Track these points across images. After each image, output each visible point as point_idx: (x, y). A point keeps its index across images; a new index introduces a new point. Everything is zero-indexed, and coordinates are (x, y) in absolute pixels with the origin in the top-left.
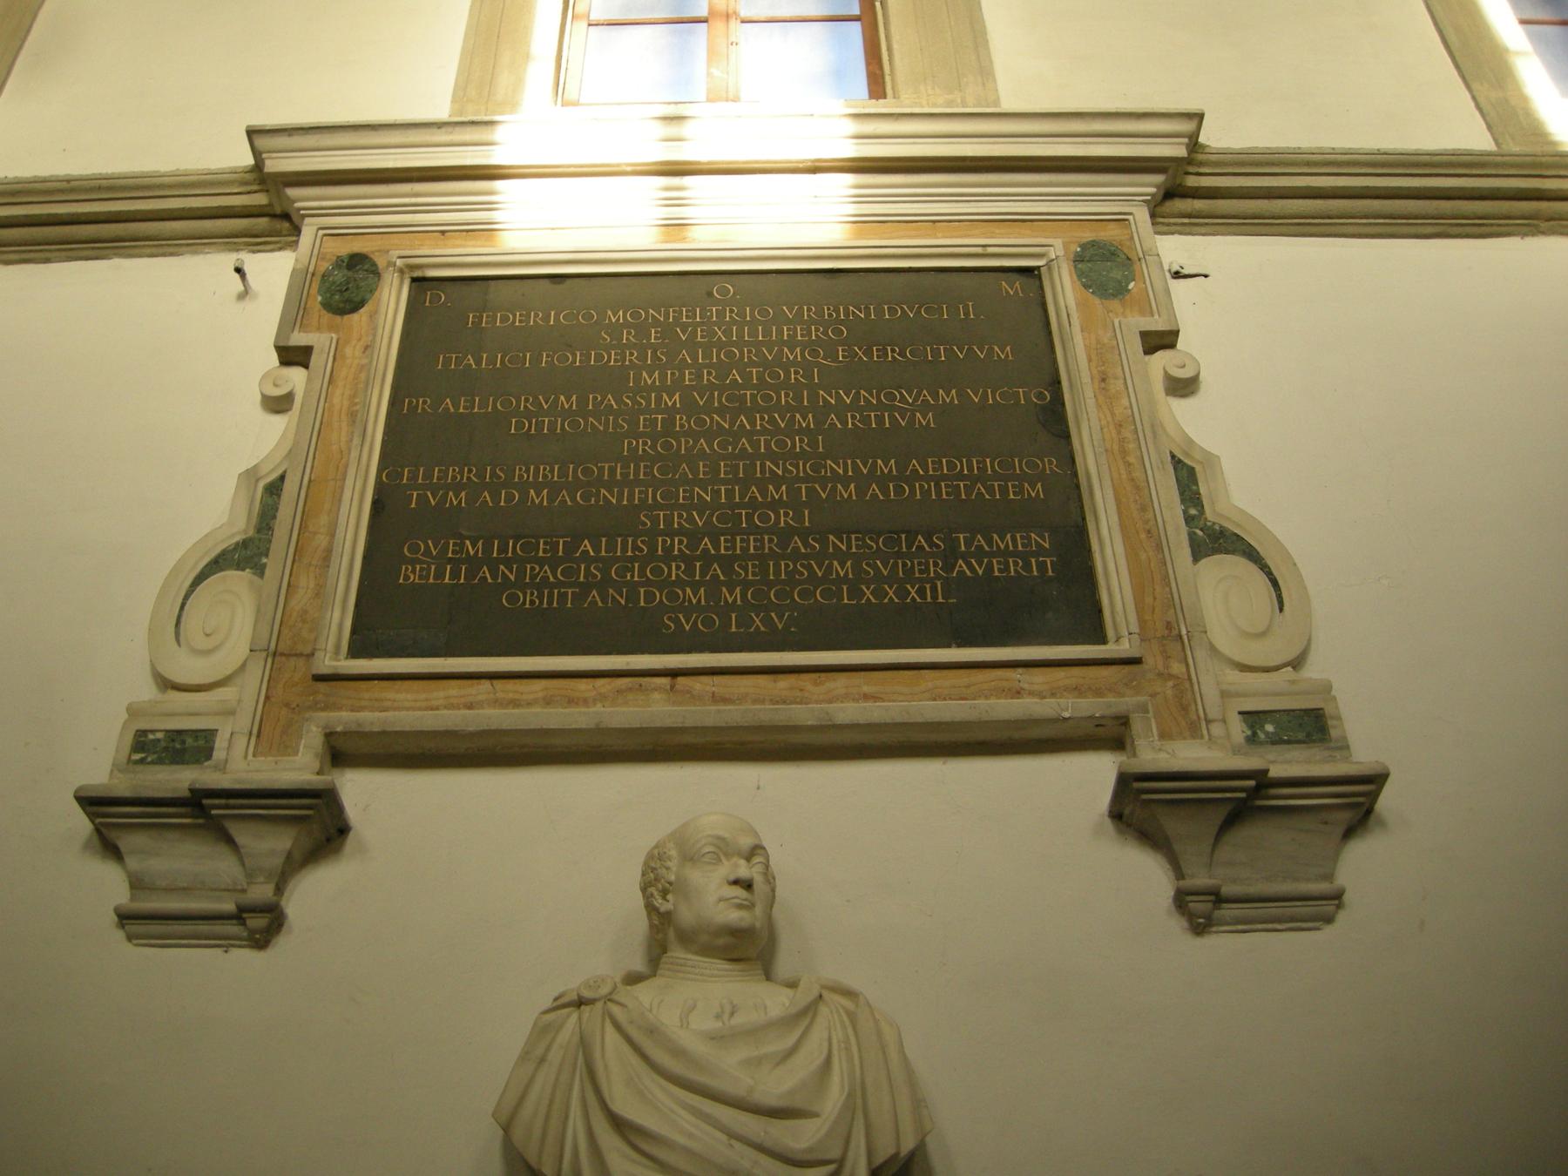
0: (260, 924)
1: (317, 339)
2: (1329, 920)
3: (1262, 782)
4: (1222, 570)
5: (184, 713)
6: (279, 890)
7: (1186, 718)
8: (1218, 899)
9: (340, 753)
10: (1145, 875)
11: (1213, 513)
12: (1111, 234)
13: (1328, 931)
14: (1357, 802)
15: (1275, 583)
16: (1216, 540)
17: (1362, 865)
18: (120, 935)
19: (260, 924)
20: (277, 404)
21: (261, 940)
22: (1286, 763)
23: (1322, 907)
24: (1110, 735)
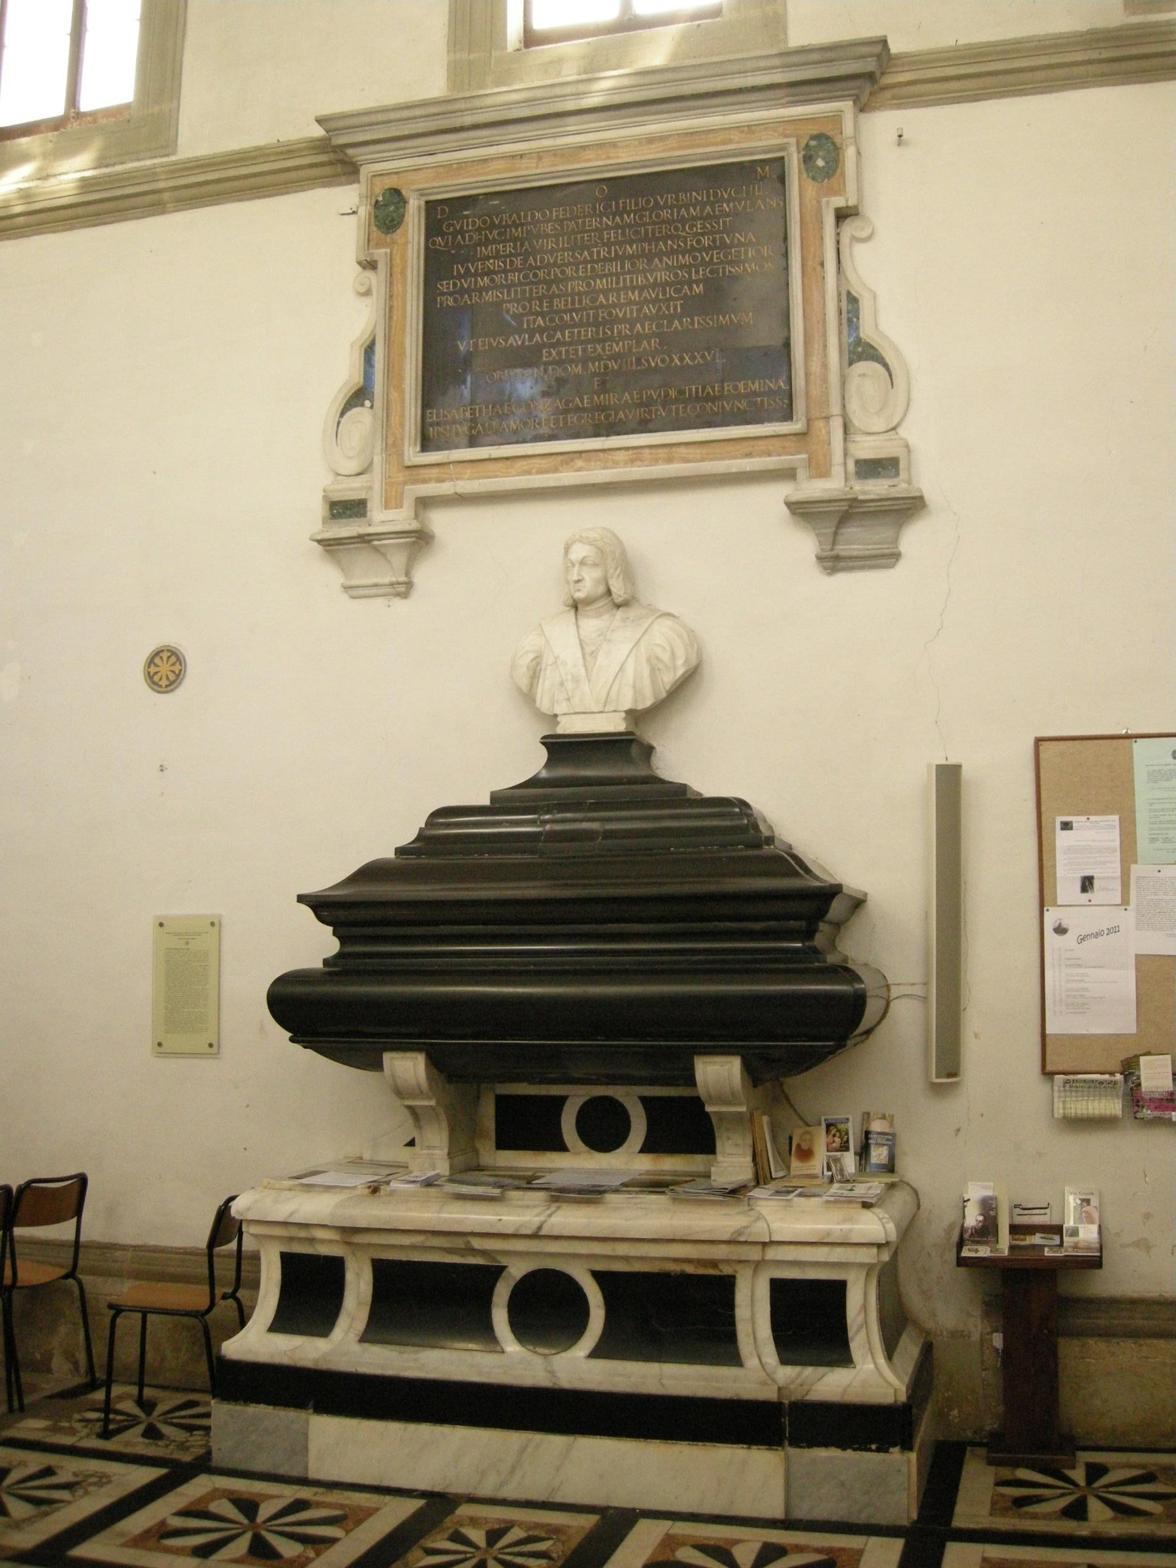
0: (404, 589)
1: (380, 254)
2: (893, 566)
3: (854, 502)
4: (862, 367)
5: (350, 490)
6: (407, 574)
7: (820, 470)
8: (837, 558)
9: (424, 503)
10: (804, 545)
11: (867, 331)
12: (828, 130)
13: (891, 572)
14: (909, 508)
15: (890, 376)
16: (862, 351)
17: (914, 539)
18: (345, 596)
19: (404, 589)
20: (368, 293)
21: (405, 595)
22: (875, 488)
23: (893, 557)
24: (788, 474)
